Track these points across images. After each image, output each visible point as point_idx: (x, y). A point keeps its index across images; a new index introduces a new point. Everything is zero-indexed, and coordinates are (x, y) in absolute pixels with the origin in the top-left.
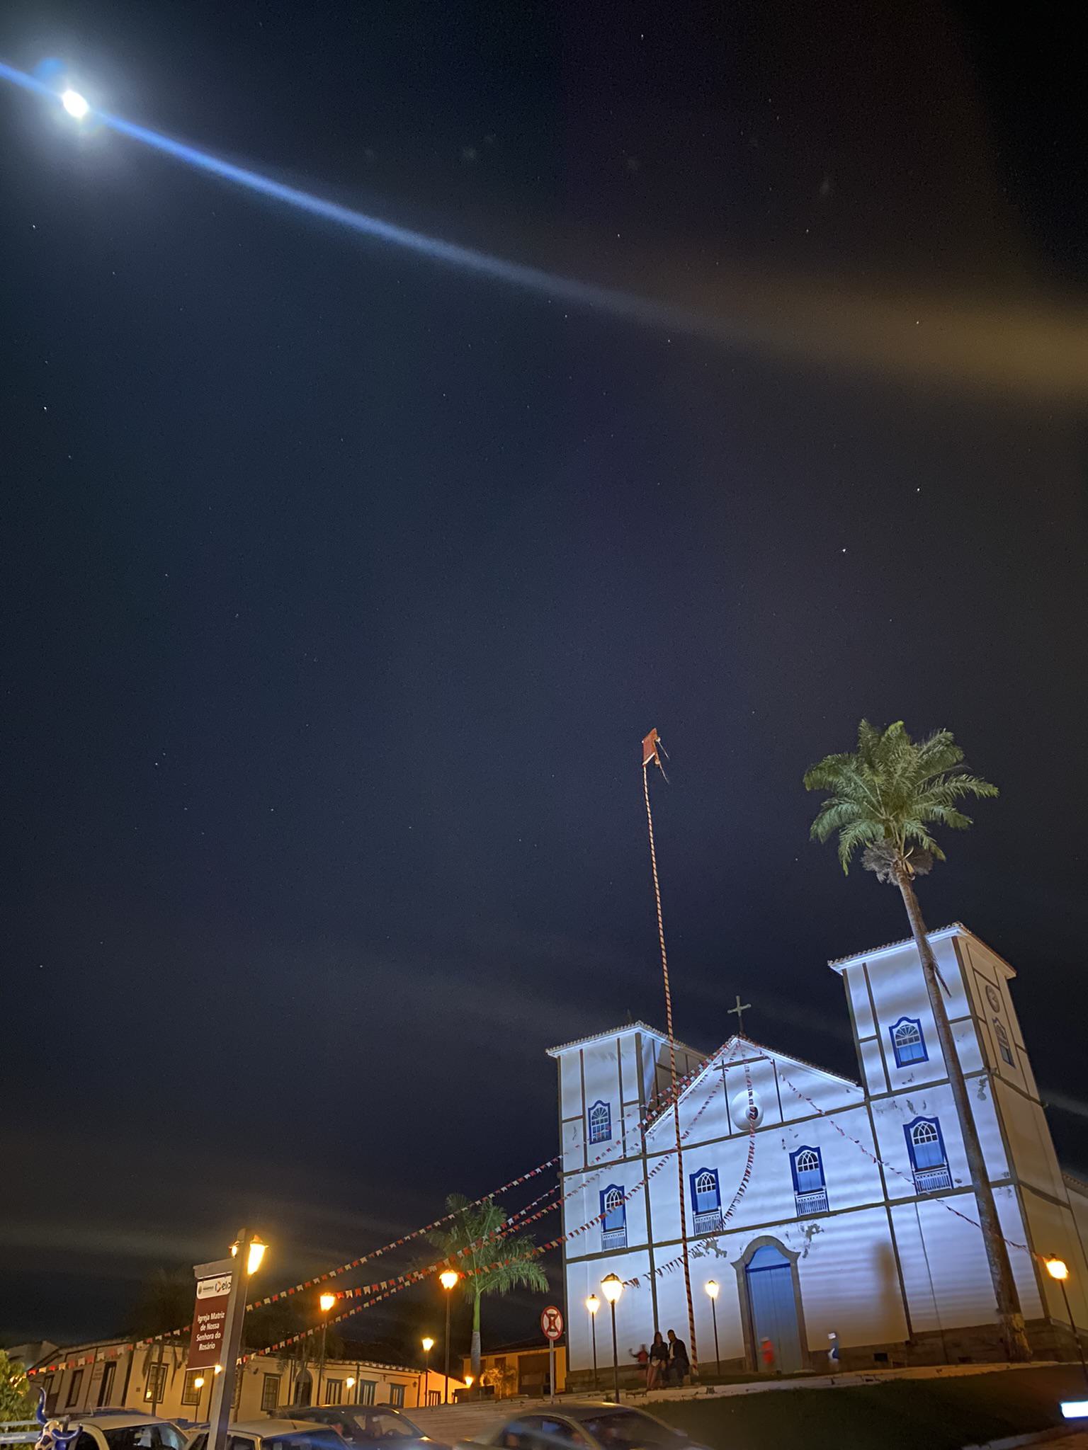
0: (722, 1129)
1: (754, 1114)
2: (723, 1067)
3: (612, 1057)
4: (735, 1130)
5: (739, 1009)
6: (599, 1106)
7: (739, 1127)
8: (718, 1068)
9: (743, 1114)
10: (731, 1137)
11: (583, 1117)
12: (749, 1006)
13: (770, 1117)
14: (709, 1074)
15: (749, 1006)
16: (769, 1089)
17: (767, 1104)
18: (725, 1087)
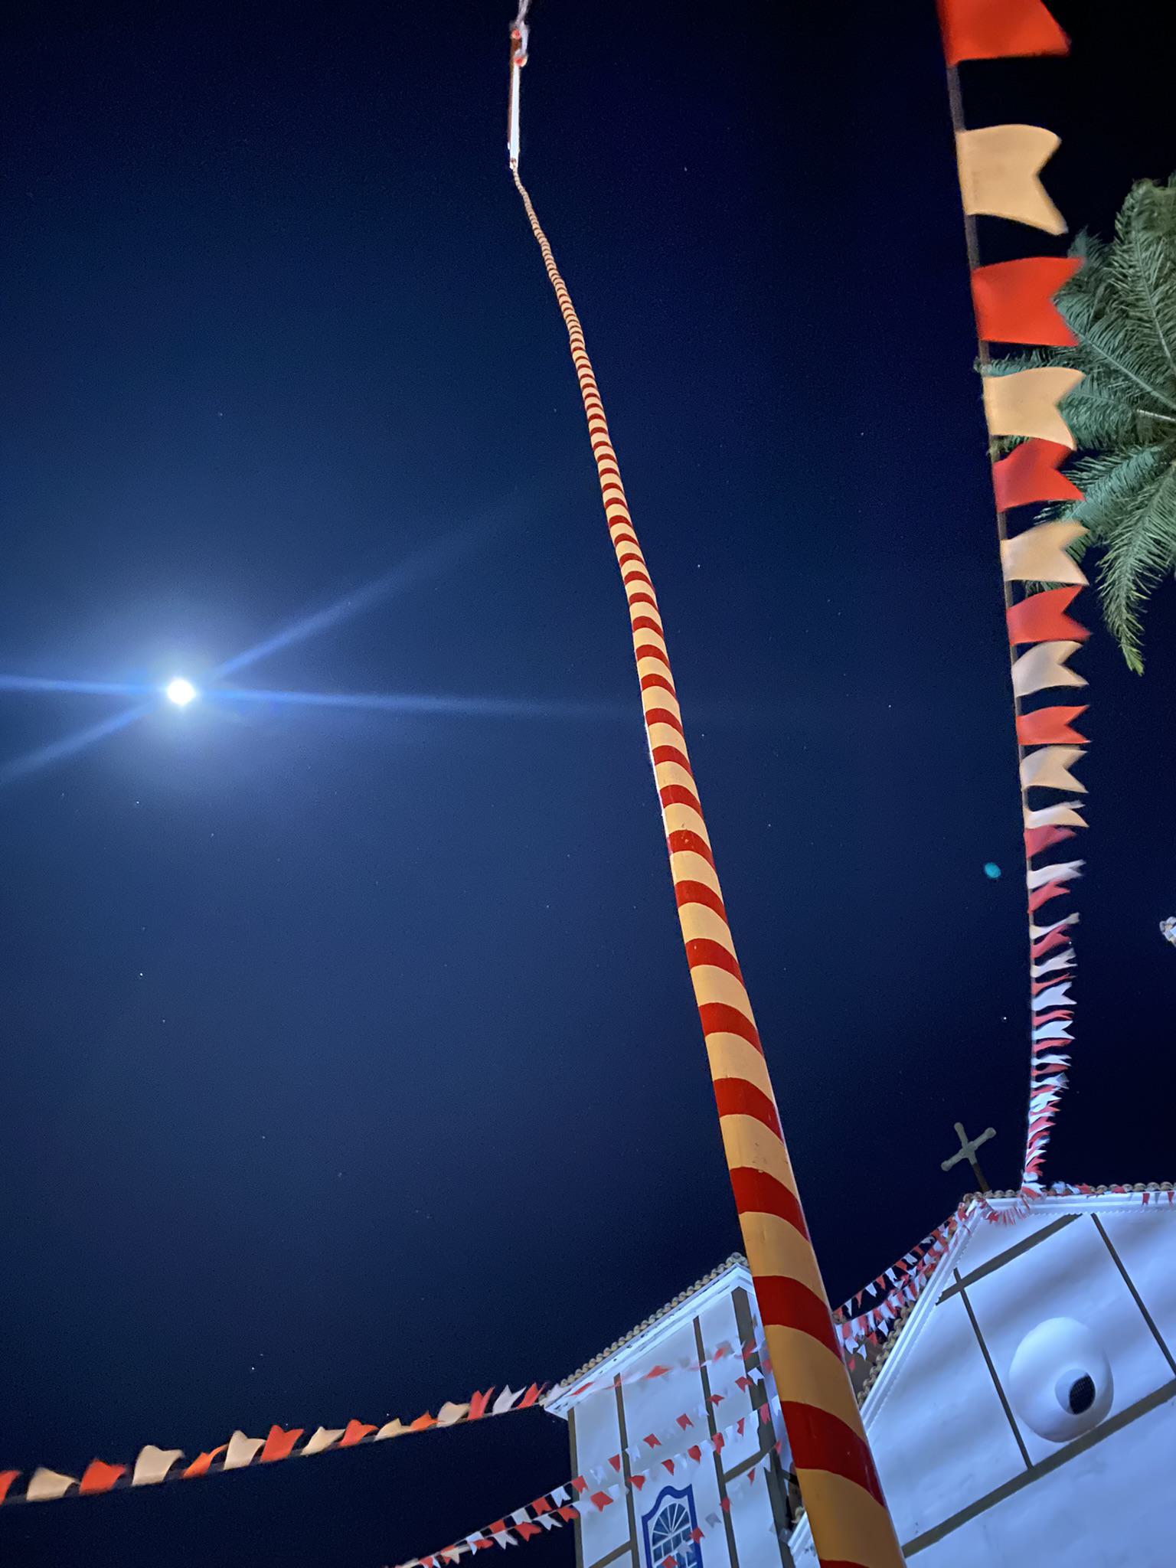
0: (998, 1458)
1: (1082, 1395)
2: (961, 1285)
3: (685, 1363)
4: (1040, 1448)
5: (968, 1150)
6: (668, 1501)
7: (1048, 1435)
8: (946, 1295)
9: (1051, 1400)
10: (1033, 1472)
11: (632, 1545)
12: (989, 1133)
13: (1137, 1373)
14: (926, 1317)
15: (989, 1133)
16: (1108, 1295)
17: (1108, 1343)
18: (980, 1336)
